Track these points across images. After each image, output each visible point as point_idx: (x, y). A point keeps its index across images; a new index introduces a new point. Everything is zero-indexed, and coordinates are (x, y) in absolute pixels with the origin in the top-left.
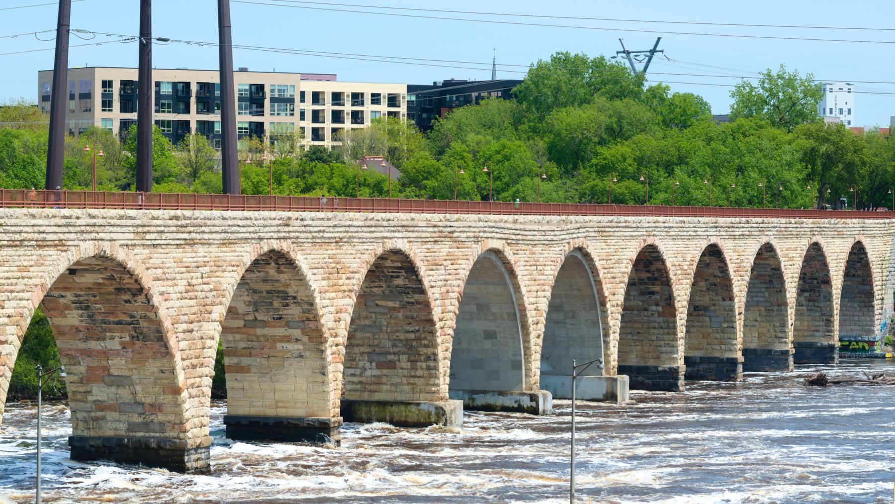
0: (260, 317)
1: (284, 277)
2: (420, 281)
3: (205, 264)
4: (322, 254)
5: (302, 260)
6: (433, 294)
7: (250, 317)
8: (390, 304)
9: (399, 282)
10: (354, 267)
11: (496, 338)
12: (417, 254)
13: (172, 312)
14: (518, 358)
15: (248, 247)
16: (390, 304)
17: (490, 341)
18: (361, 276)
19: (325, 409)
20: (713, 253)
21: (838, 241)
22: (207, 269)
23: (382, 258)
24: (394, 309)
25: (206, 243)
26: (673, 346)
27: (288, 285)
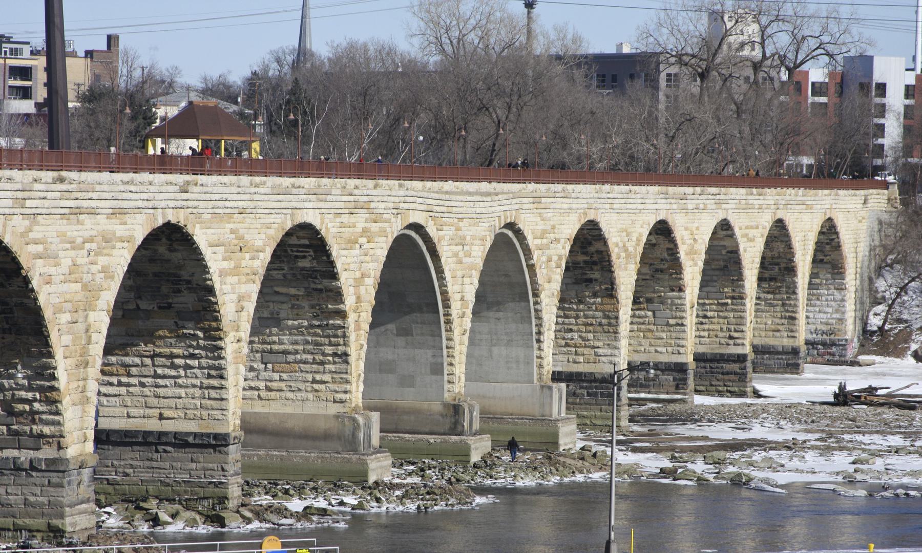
0: (144, 305)
1: (177, 257)
2: (332, 264)
3: (91, 240)
4: (224, 231)
5: (201, 237)
6: (345, 280)
7: (132, 306)
8: (293, 291)
9: (305, 263)
10: (259, 243)
11: (412, 335)
12: (330, 230)
13: (55, 300)
14: (439, 360)
15: (140, 218)
16: (293, 291)
17: (403, 338)
18: (266, 256)
19: (223, 421)
20: (662, 230)
21: (806, 217)
22: (94, 246)
23: (288, 234)
24: (296, 297)
25: (93, 212)
26: (616, 348)
27: (180, 267)
